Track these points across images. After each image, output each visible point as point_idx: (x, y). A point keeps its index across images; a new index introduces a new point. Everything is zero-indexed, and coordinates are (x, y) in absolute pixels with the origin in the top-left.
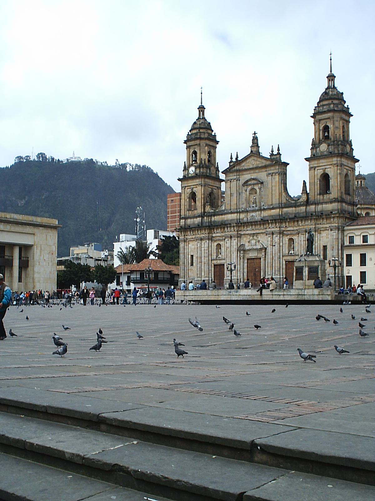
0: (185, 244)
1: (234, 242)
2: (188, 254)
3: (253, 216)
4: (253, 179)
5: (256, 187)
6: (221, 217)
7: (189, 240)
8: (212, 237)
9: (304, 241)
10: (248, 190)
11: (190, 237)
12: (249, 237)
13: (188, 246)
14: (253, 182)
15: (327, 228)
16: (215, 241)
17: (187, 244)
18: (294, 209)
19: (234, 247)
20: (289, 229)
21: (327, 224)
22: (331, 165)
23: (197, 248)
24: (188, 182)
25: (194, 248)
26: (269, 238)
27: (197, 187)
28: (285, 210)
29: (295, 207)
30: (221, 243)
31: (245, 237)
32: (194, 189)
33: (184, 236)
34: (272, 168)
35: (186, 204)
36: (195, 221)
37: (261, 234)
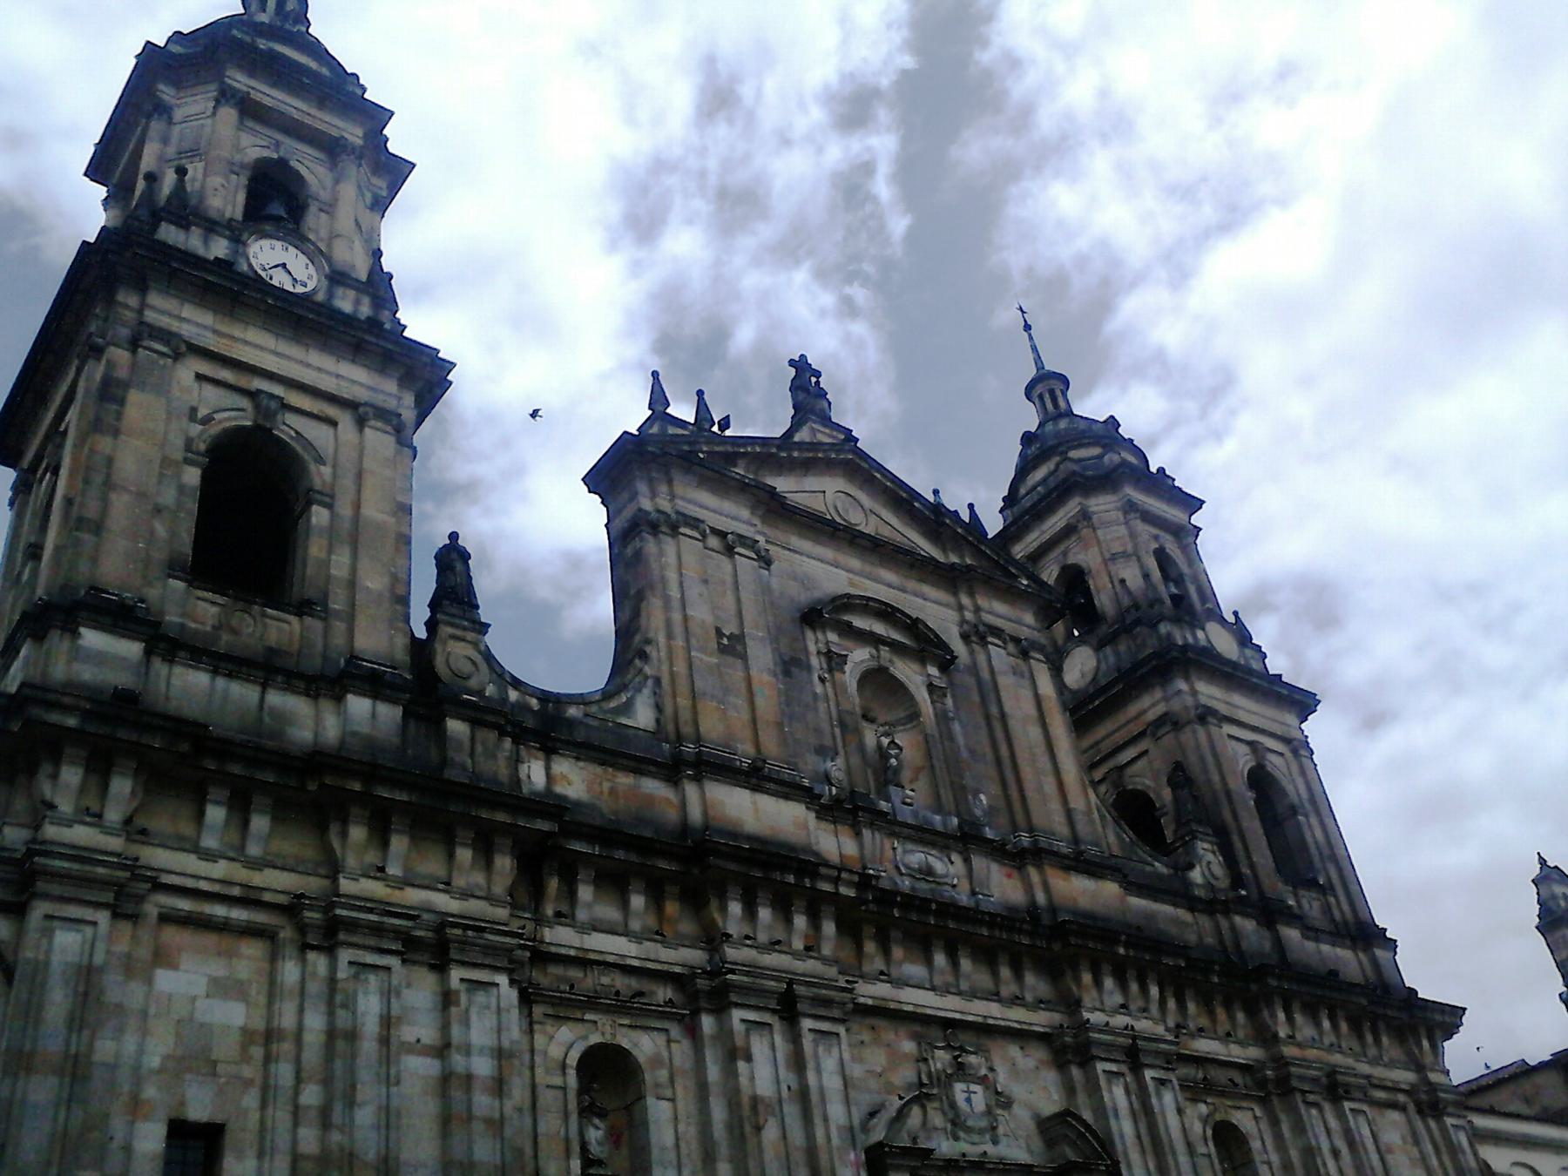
0: (122, 947)
1: (830, 1063)
2: (136, 1107)
3: (928, 871)
4: (887, 613)
5: (909, 673)
6: (625, 780)
7: (185, 905)
8: (542, 957)
9: (1336, 1153)
10: (847, 668)
11: (220, 869)
12: (909, 1046)
13: (149, 981)
14: (879, 628)
15: (1395, 1089)
16: (569, 1006)
17: (144, 953)
18: (1185, 915)
19: (836, 1111)
20: (1204, 1046)
21: (1391, 1065)
22: (1287, 741)
23: (352, 1036)
24: (237, 331)
25: (247, 1035)
26: (1119, 1092)
27: (333, 423)
28: (1137, 902)
29: (1192, 910)
30: (643, 1045)
31: (877, 1041)
32: (291, 419)
33: (133, 829)
34: (1000, 607)
35: (168, 497)
36: (282, 718)
37: (1014, 1050)
